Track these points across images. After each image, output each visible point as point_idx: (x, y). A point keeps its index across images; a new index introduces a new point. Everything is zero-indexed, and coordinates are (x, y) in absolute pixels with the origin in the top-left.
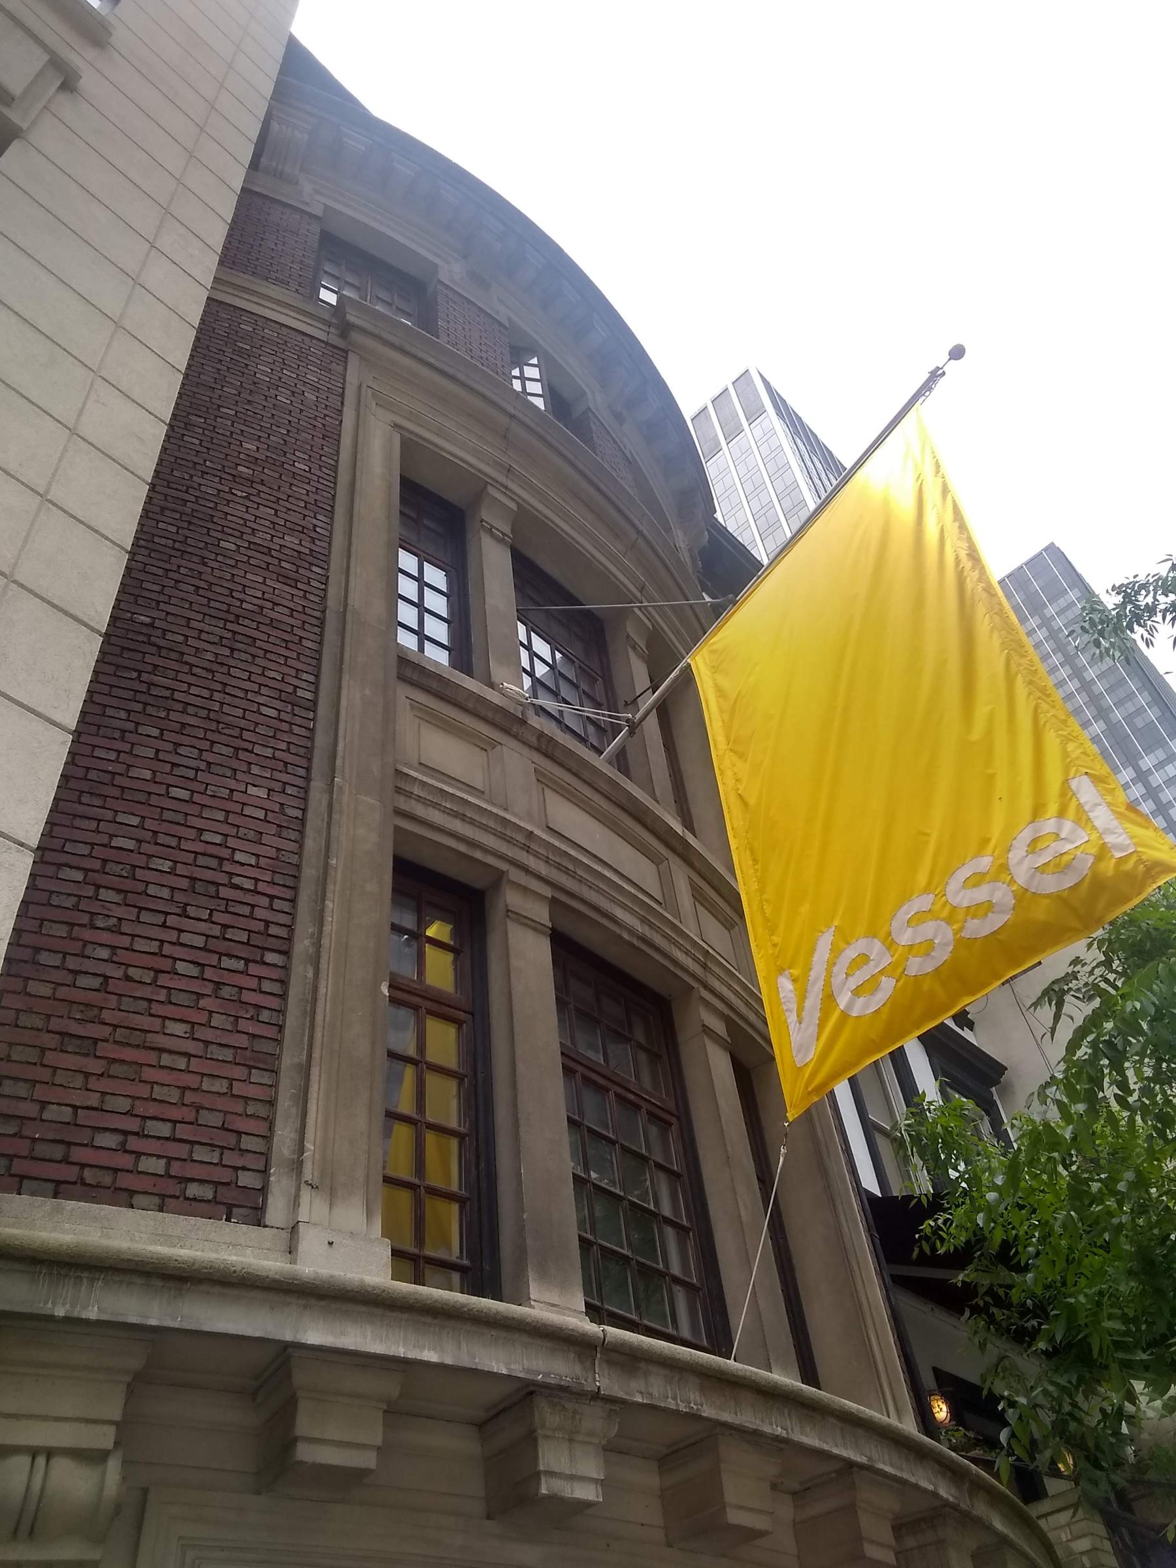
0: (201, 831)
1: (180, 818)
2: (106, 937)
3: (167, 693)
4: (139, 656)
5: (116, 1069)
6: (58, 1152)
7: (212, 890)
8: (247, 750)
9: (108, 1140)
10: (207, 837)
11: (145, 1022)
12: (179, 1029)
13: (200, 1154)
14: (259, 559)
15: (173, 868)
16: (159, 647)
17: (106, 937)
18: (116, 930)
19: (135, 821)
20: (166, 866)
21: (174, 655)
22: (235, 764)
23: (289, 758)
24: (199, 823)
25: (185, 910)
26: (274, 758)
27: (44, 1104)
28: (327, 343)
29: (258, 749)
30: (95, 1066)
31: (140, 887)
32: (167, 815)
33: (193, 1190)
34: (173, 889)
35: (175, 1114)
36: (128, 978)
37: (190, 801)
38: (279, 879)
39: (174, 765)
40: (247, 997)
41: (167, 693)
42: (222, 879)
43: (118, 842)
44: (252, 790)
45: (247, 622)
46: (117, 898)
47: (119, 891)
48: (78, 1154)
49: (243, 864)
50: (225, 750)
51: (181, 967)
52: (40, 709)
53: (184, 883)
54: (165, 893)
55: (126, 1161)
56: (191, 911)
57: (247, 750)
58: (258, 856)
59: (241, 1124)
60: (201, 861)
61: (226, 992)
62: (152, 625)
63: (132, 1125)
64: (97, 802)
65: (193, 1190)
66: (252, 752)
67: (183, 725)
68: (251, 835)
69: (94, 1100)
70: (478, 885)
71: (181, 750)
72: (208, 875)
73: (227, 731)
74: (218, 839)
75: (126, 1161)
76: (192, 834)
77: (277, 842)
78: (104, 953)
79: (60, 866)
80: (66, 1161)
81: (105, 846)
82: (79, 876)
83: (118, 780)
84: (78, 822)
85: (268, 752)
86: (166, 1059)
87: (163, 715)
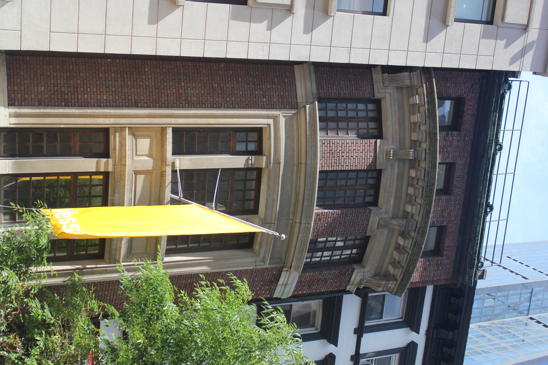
2: (59, 75)
5: (32, 80)
6: (15, 74)
9: (19, 81)
11: (43, 83)
12: (43, 89)
13: (19, 95)
17: (59, 75)
18: (60, 76)
21: (138, 77)
27: (23, 71)
28: (297, 103)
30: (32, 77)
32: (91, 81)
33: (13, 95)
35: (26, 90)
36: (51, 79)
40: (53, 100)
48: (15, 77)
51: (56, 88)
53: (76, 86)
54: (72, 83)
55: (16, 84)
56: (69, 88)
59: (26, 101)
61: (53, 96)
63: (22, 84)
65: (13, 95)
69: (25, 78)
70: (110, 156)
75: (16, 84)
76: (88, 86)
78: (55, 75)
80: (14, 75)
83: (97, 72)
86: (36, 88)
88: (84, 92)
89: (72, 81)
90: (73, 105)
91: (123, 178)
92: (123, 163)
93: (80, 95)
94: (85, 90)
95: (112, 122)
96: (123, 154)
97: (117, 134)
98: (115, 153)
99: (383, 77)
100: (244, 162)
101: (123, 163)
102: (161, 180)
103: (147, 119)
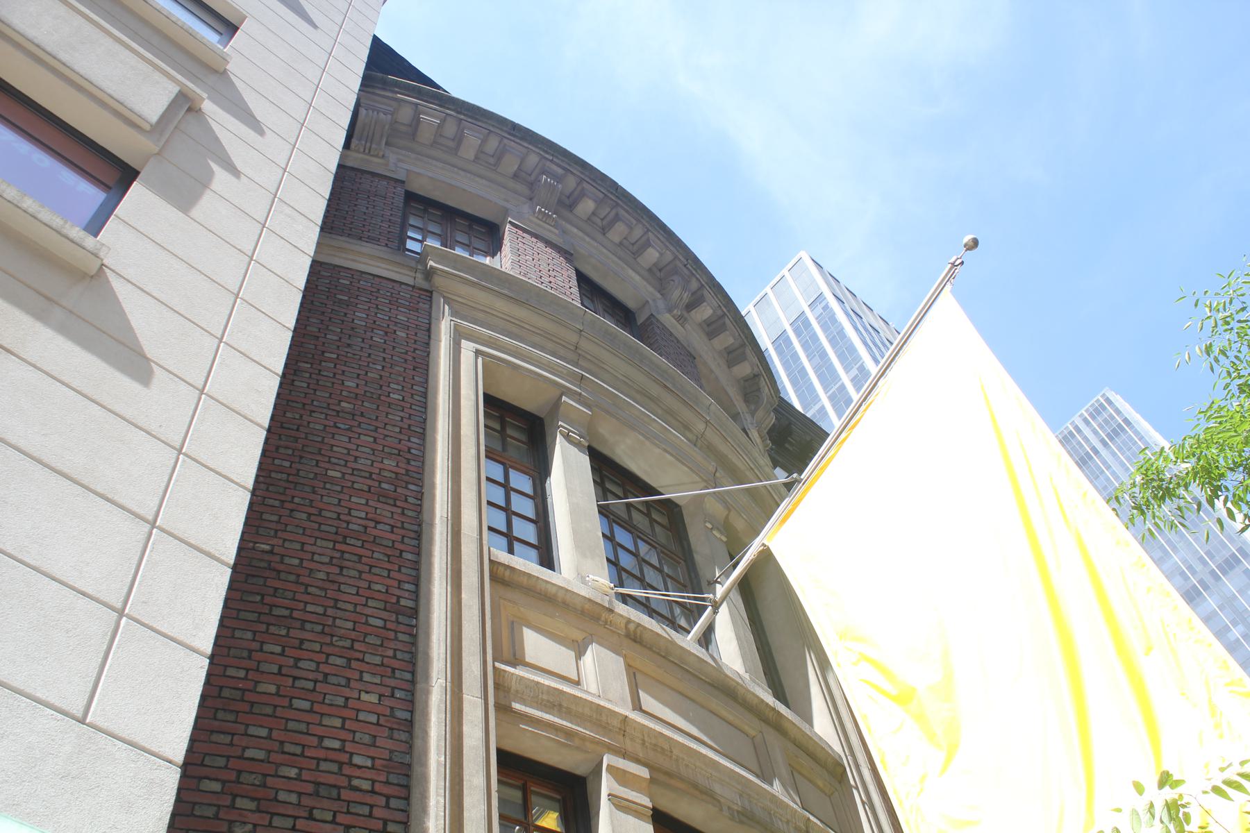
0: (321, 738)
1: (303, 727)
3: (286, 613)
4: (261, 581)
7: (334, 793)
8: (358, 660)
10: (328, 743)
14: (361, 484)
15: (299, 774)
16: (279, 572)
19: (264, 732)
20: (293, 773)
21: (292, 578)
22: (348, 674)
23: (396, 664)
24: (319, 731)
25: (311, 813)
26: (382, 665)
28: (413, 287)
29: (368, 658)
31: (272, 794)
32: (291, 725)
34: (300, 794)
37: (311, 711)
38: (393, 779)
39: (295, 678)
41: (286, 613)
42: (343, 781)
43: (249, 753)
44: (364, 697)
45: (352, 541)
46: (252, 805)
47: (253, 799)
49: (360, 767)
50: (339, 661)
52: (181, 638)
53: (310, 788)
54: (293, 798)
56: (317, 814)
57: (358, 660)
58: (373, 758)
60: (324, 766)
62: (271, 552)
64: (231, 717)
66: (363, 661)
67: (302, 641)
68: (367, 739)
70: (580, 771)
71: (301, 664)
72: (331, 779)
73: (341, 643)
74: (337, 745)
76: (315, 741)
77: (389, 744)
79: (201, 778)
81: (239, 758)
82: (216, 787)
84: (215, 737)
85: (377, 660)
87: (283, 632)
88: (341, 764)
89: (282, 796)
90: (400, 816)
91: (666, 747)
92: (616, 723)
93: (356, 782)
94: (331, 755)
95: (480, 702)
96: (587, 711)
97: (517, 706)
98: (583, 738)
99: (358, 151)
100: (574, 451)
101: (616, 723)
102: (650, 649)
103: (463, 596)
